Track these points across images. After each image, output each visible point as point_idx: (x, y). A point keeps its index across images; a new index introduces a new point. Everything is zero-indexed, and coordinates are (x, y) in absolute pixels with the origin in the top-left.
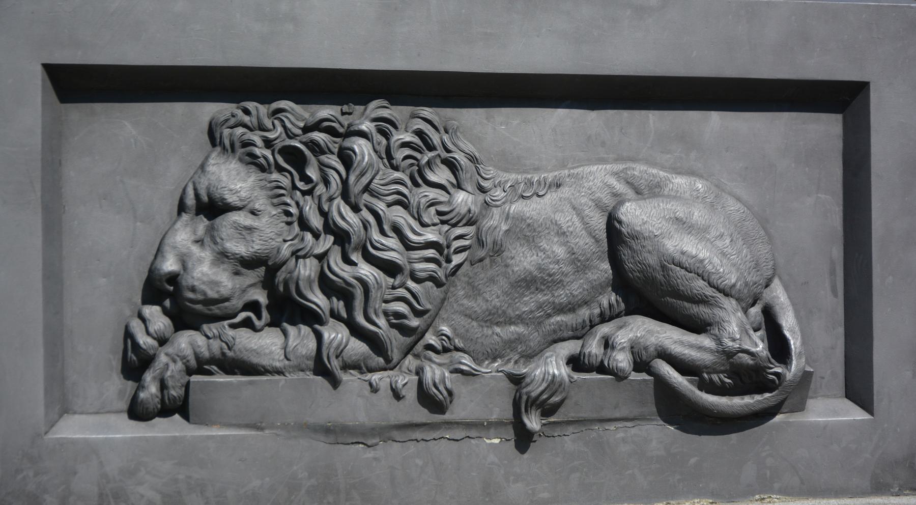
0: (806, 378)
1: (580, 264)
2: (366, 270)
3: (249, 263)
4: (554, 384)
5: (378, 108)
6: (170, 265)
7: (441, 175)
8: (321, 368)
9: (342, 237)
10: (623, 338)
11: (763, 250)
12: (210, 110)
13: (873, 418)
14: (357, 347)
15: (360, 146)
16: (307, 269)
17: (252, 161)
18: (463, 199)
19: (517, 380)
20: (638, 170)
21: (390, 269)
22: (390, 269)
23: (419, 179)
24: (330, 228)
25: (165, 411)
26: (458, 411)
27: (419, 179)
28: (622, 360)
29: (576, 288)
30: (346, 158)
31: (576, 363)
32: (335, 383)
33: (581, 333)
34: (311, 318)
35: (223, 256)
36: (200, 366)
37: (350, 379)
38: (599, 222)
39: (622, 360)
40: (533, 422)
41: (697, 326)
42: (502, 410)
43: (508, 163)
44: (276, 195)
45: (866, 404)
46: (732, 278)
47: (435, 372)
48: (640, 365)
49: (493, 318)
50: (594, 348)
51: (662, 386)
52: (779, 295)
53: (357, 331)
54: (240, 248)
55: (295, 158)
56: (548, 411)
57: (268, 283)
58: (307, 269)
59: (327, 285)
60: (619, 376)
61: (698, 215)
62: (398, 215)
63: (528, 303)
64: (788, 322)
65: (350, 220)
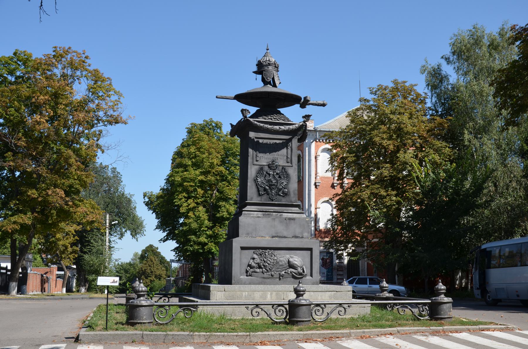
0: (306, 274)
1: (285, 264)
2: (267, 264)
3: (256, 263)
4: (283, 274)
5: (268, 250)
6: (250, 263)
7: (273, 256)
8: (263, 272)
9: (265, 262)
10: (289, 270)
11: (303, 263)
12: (253, 251)
13: (311, 278)
14: (266, 271)
15: (266, 254)
16: (262, 264)
17: (257, 255)
18: (275, 258)
19: (280, 274)
20: (291, 255)
21: (269, 264)
22: (269, 264)
23: (271, 256)
24: (264, 260)
25: (251, 275)
26: (274, 277)
27: (271, 256)
28: (289, 272)
29: (285, 266)
30: (265, 254)
31: (285, 273)
32: (264, 274)
33: (286, 270)
34: (262, 268)
35: (255, 263)
36: (253, 272)
37: (265, 273)
38: (287, 260)
39: (289, 272)
40: (281, 277)
41: (296, 269)
42: (278, 276)
43: (279, 255)
44: (259, 258)
45: (312, 277)
46: (299, 265)
47: (272, 273)
48: (291, 273)
49: (278, 268)
50: (287, 271)
51: (293, 275)
52: (304, 267)
53: (266, 269)
54: (256, 262)
55: (261, 255)
56: (282, 277)
57: (258, 265)
58: (262, 264)
59: (263, 265)
60: (289, 274)
61: (296, 260)
62: (270, 259)
63: (281, 267)
64: (305, 269)
65: (265, 260)
